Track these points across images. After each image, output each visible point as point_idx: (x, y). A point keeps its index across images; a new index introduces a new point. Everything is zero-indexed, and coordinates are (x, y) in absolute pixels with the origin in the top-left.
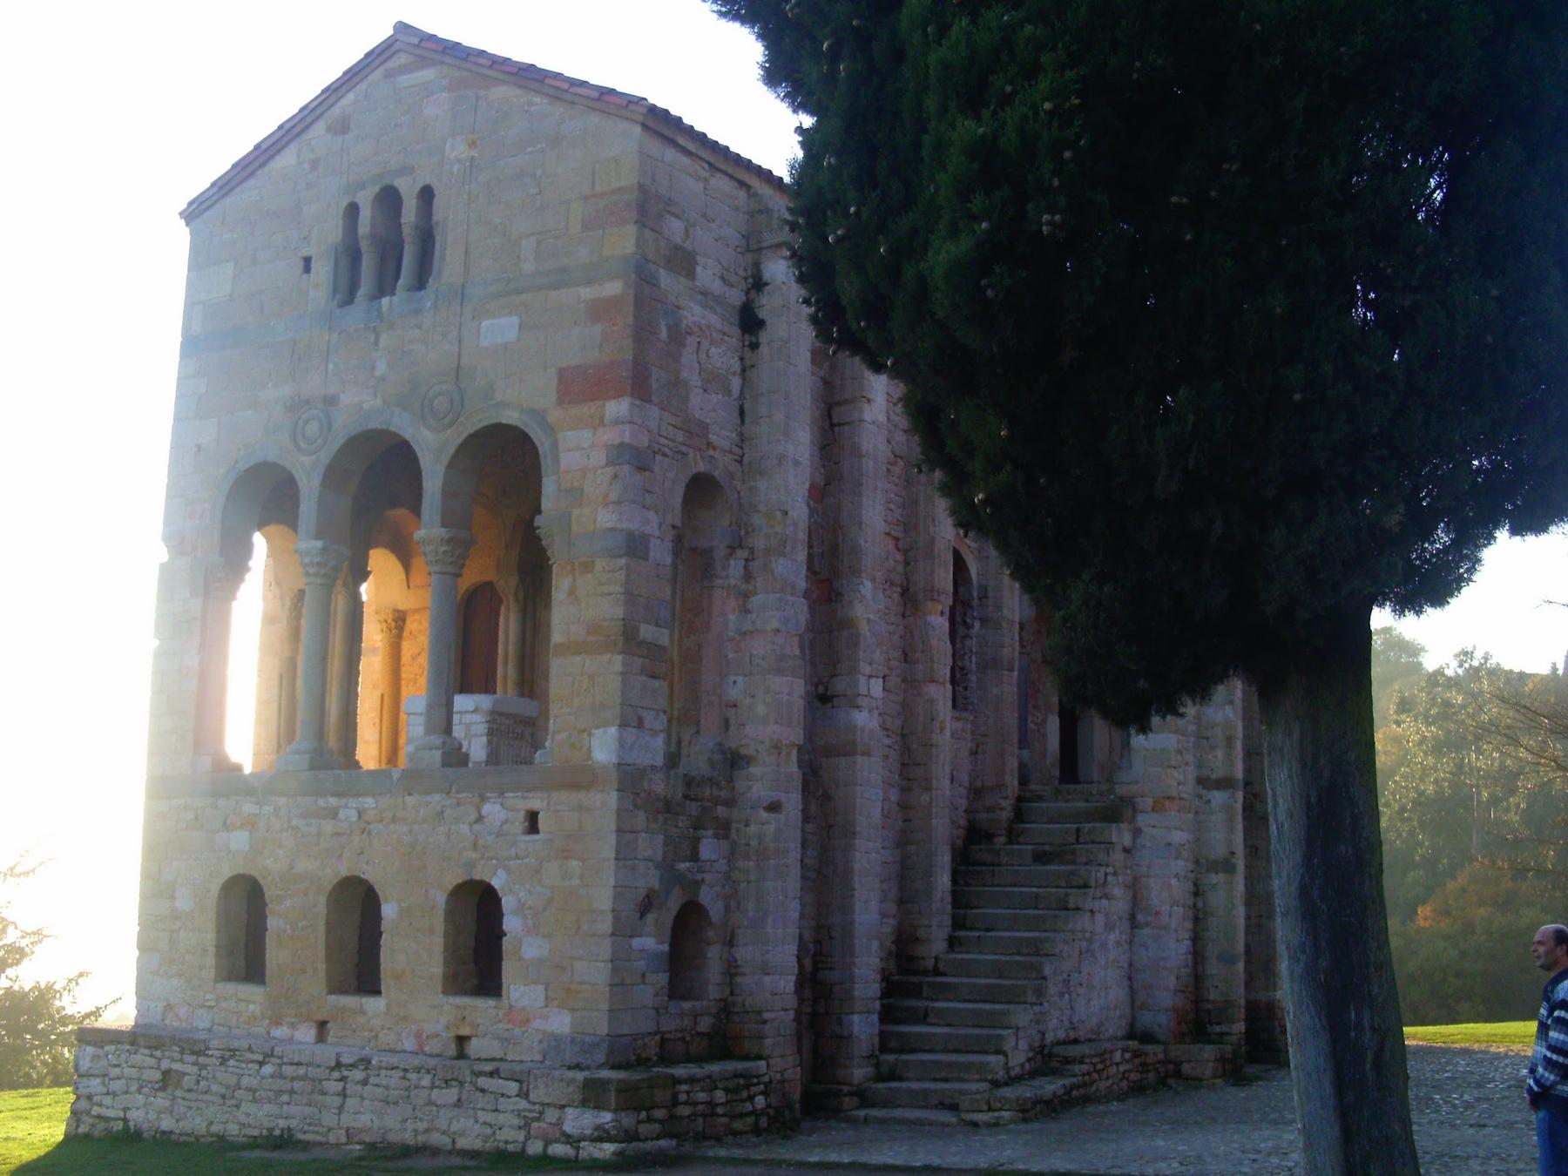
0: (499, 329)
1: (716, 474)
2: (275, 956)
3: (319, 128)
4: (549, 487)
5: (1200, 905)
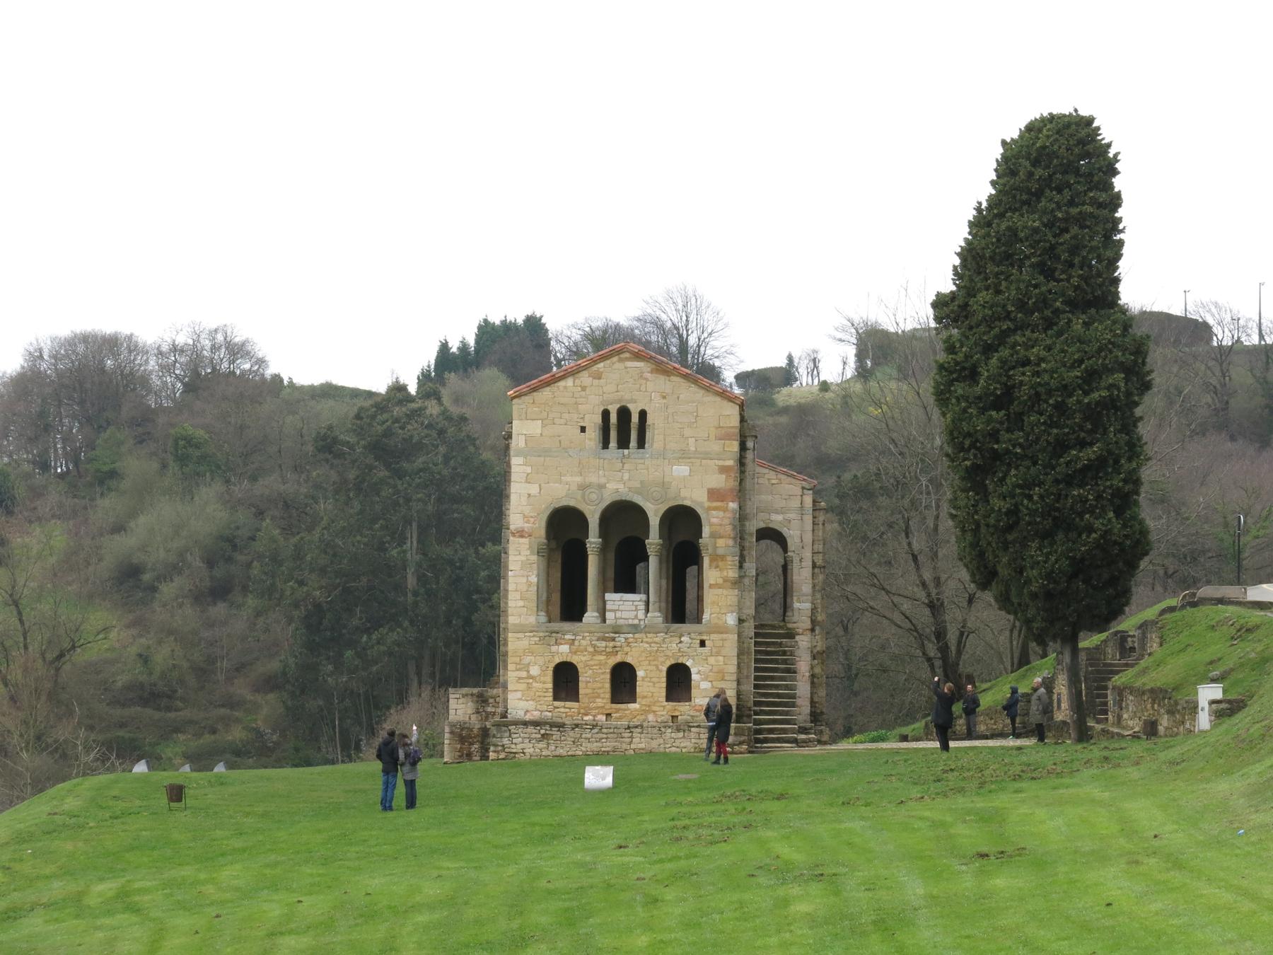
0: (681, 470)
2: (583, 690)
3: (585, 374)
4: (706, 531)
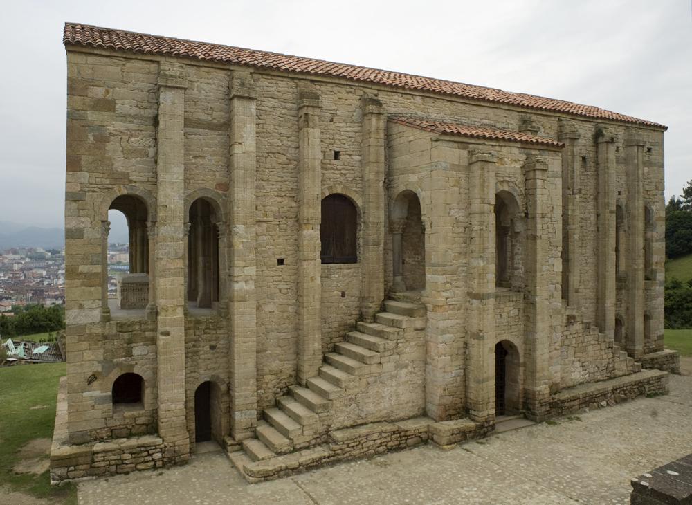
1: (138, 193)
5: (468, 353)
